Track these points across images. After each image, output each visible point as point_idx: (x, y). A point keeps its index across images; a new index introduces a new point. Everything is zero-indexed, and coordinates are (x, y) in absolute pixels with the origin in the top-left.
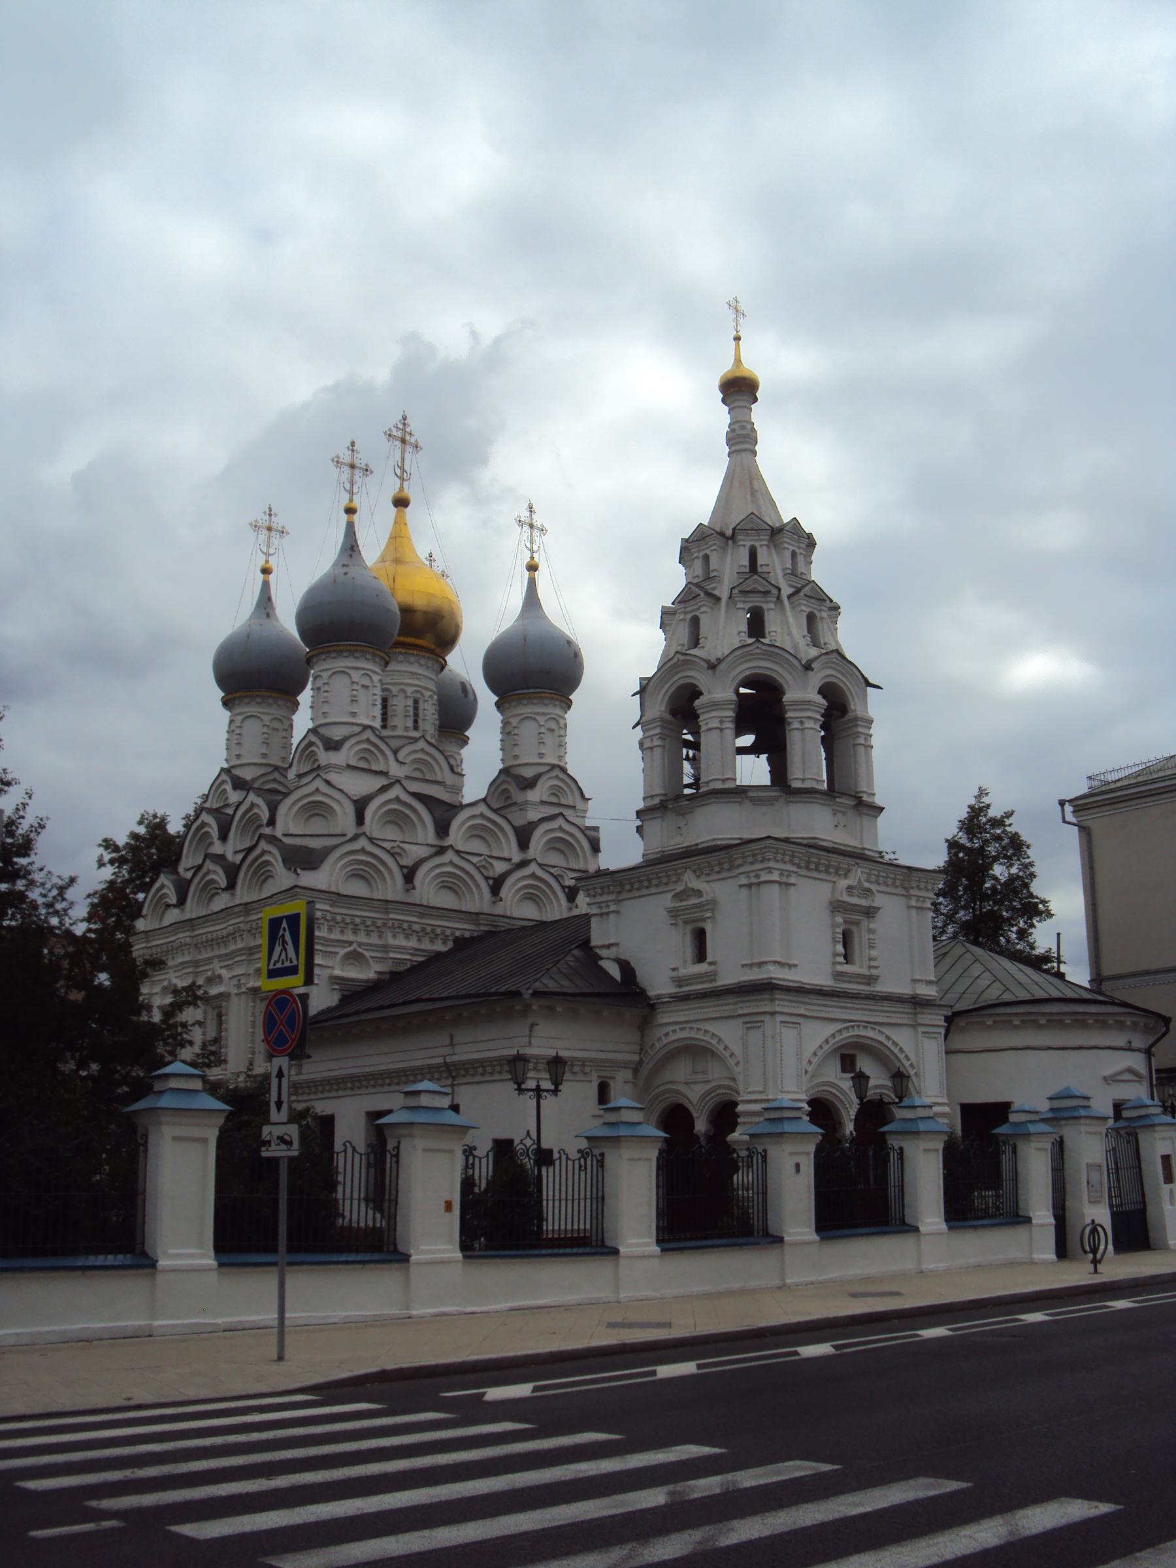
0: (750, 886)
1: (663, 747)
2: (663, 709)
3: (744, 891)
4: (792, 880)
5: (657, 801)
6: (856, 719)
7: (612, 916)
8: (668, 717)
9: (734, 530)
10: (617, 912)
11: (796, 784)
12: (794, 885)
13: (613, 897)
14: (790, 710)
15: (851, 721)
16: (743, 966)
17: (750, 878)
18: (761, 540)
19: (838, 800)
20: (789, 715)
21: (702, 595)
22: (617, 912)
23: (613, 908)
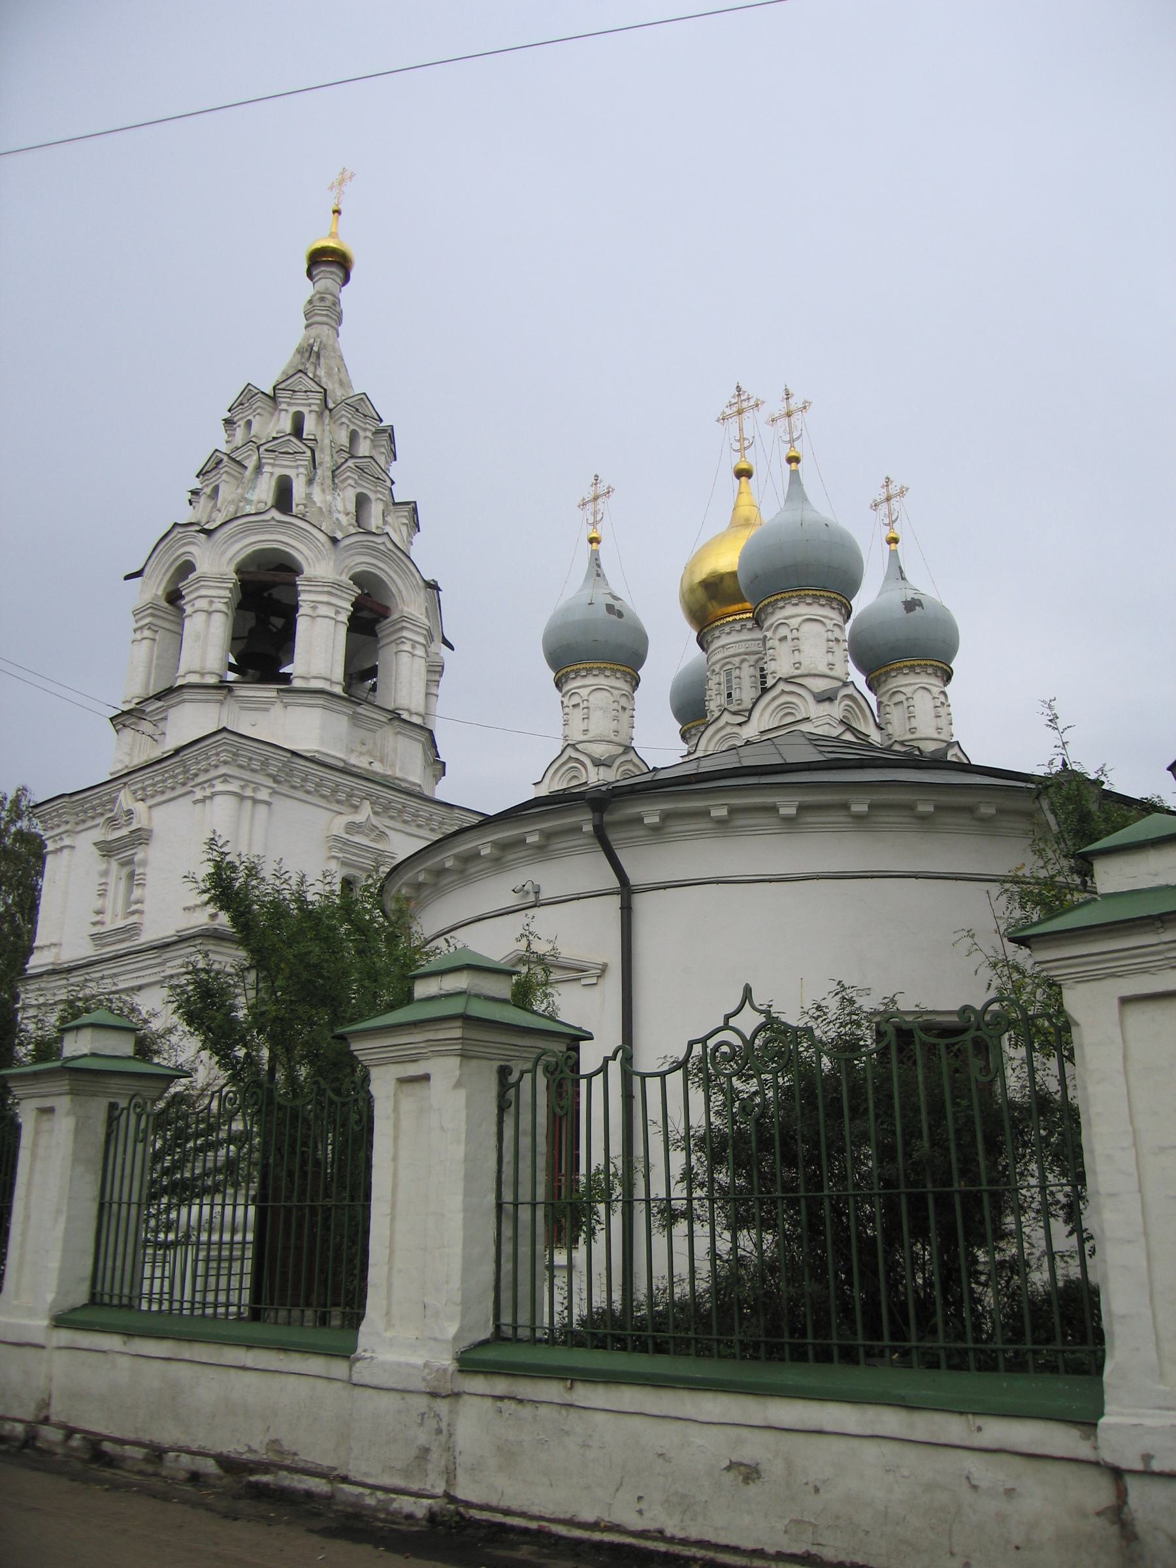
0: (203, 800)
1: (154, 640)
2: (160, 593)
3: (199, 805)
4: (263, 795)
5: (132, 706)
6: (403, 618)
7: (66, 851)
8: (166, 605)
9: (274, 388)
10: (72, 847)
11: (297, 683)
12: (268, 803)
13: (68, 827)
14: (304, 591)
15: (396, 622)
16: (184, 909)
17: (205, 789)
18: (310, 405)
19: (359, 710)
20: (302, 597)
21: (225, 458)
22: (72, 847)
23: (67, 841)
